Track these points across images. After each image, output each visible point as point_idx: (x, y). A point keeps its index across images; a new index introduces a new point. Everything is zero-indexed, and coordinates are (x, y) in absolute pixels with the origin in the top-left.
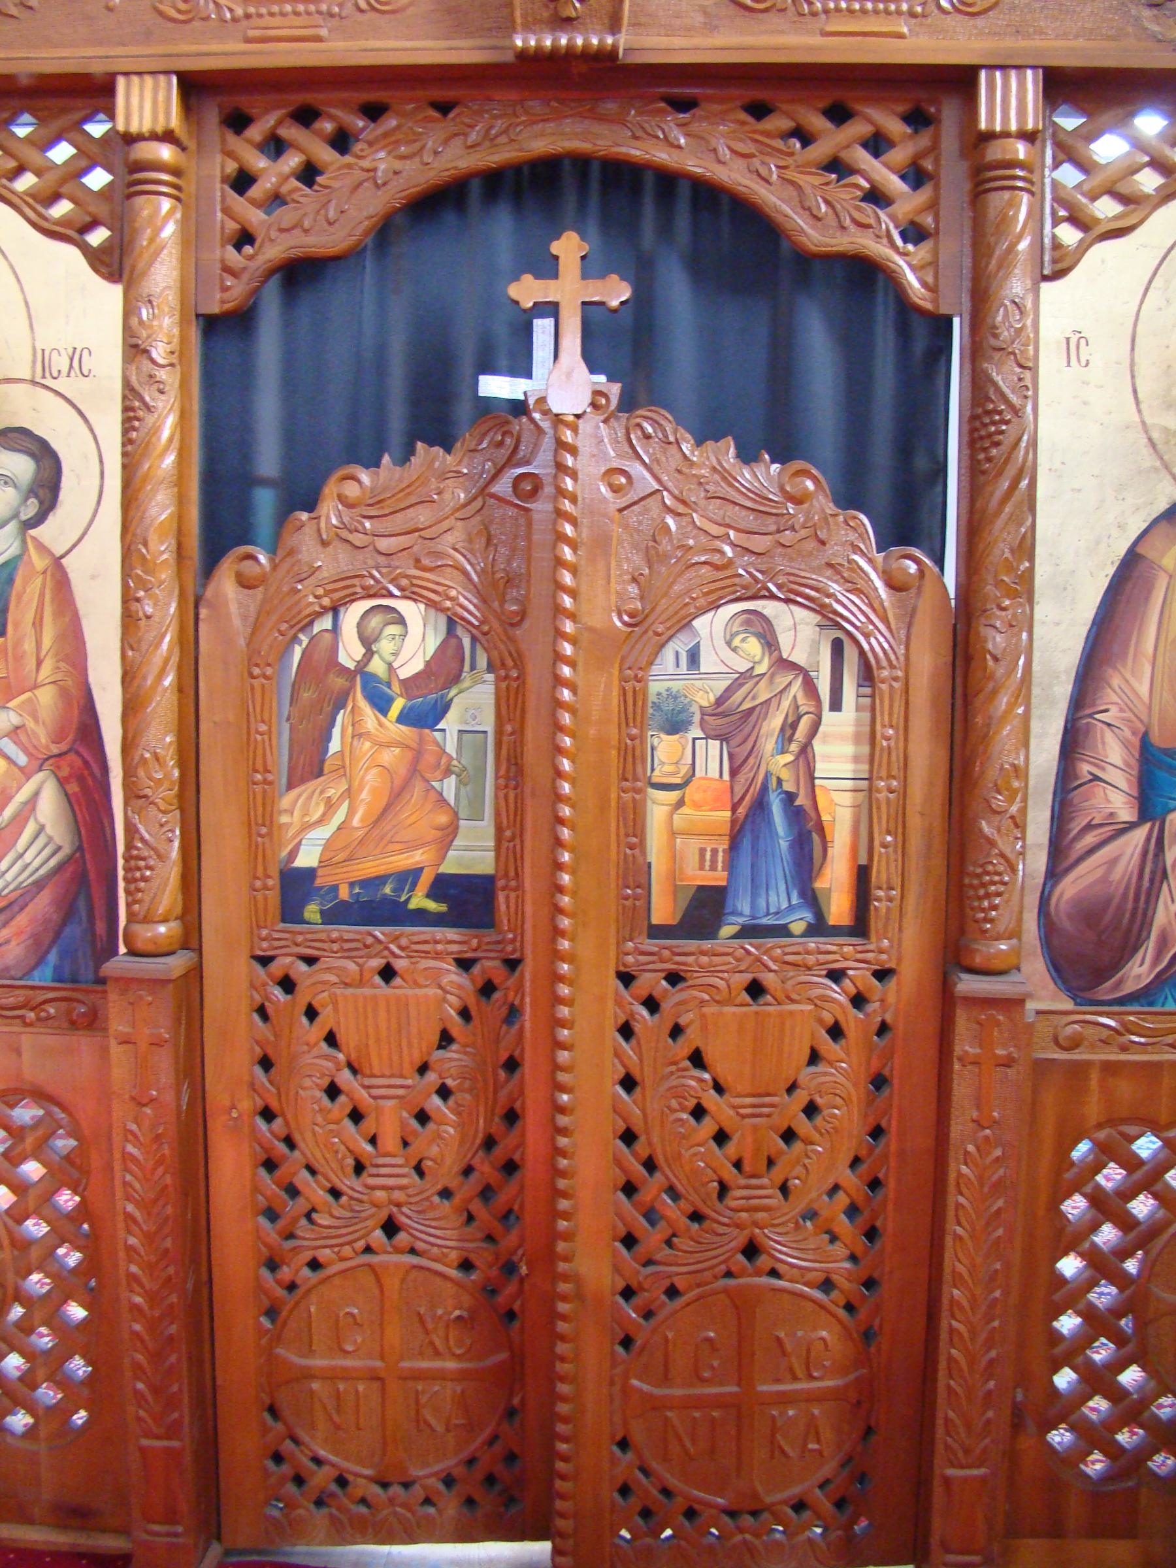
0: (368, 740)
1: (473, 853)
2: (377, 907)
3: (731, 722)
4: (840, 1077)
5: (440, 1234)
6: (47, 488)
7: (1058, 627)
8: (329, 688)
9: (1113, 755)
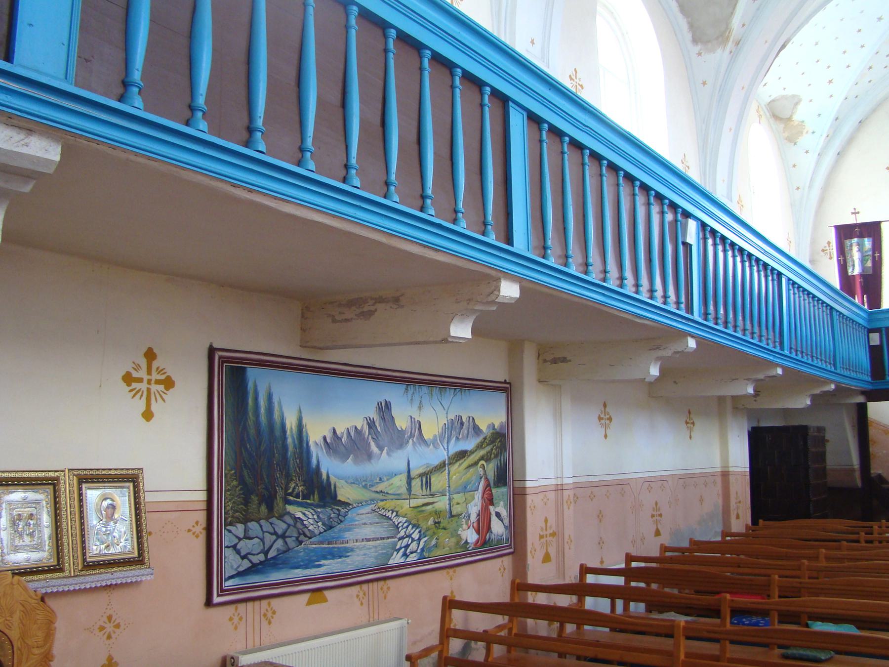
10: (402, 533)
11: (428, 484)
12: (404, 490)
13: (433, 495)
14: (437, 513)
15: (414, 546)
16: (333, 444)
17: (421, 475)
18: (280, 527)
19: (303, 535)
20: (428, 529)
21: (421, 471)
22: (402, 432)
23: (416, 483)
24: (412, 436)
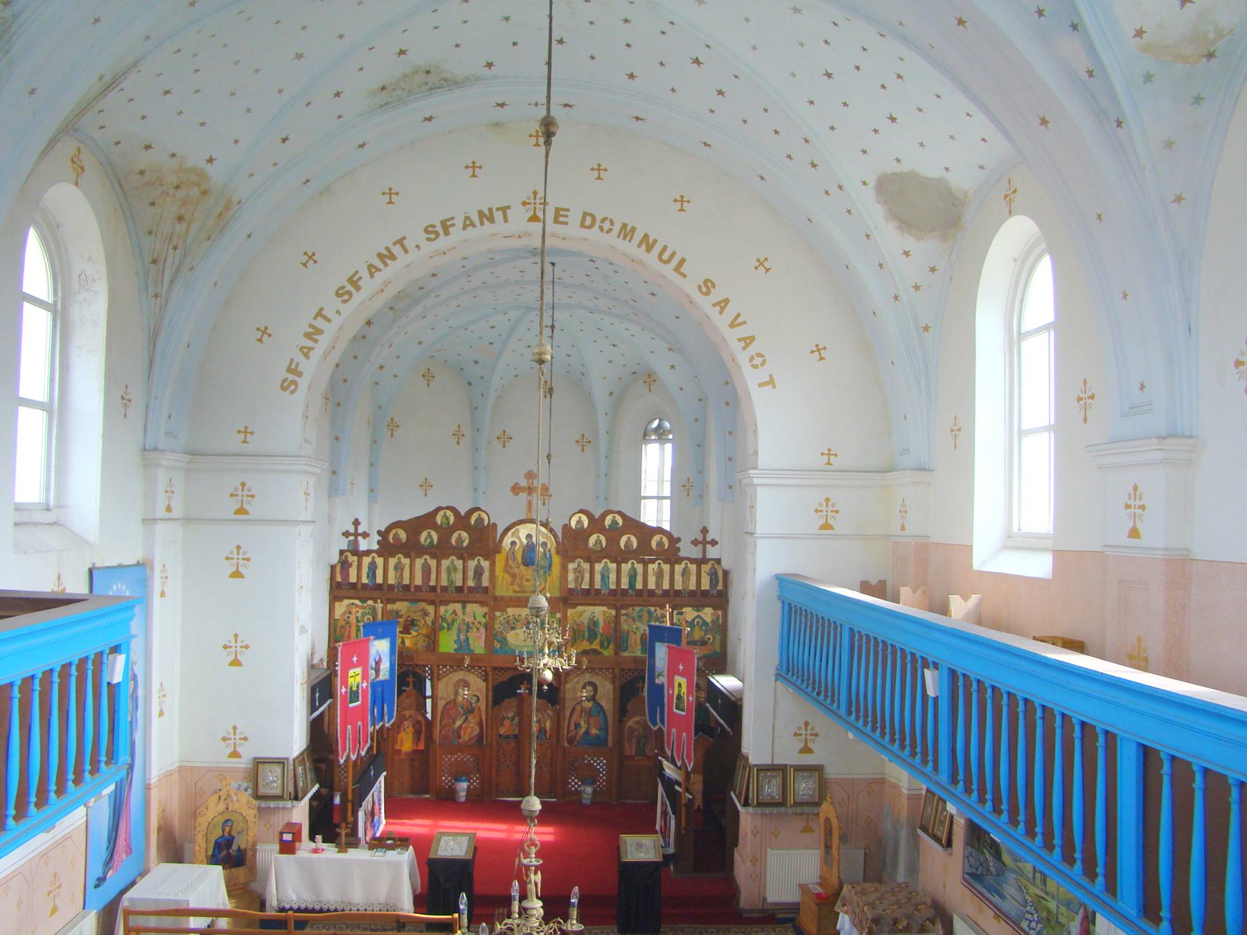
0: (507, 722)
2: (508, 737)
4: (549, 752)
6: (478, 700)
7: (568, 713)
8: (504, 718)
11: (1044, 882)
12: (1031, 876)
13: (1047, 893)
14: (1048, 910)
15: (1033, 924)
19: (988, 872)
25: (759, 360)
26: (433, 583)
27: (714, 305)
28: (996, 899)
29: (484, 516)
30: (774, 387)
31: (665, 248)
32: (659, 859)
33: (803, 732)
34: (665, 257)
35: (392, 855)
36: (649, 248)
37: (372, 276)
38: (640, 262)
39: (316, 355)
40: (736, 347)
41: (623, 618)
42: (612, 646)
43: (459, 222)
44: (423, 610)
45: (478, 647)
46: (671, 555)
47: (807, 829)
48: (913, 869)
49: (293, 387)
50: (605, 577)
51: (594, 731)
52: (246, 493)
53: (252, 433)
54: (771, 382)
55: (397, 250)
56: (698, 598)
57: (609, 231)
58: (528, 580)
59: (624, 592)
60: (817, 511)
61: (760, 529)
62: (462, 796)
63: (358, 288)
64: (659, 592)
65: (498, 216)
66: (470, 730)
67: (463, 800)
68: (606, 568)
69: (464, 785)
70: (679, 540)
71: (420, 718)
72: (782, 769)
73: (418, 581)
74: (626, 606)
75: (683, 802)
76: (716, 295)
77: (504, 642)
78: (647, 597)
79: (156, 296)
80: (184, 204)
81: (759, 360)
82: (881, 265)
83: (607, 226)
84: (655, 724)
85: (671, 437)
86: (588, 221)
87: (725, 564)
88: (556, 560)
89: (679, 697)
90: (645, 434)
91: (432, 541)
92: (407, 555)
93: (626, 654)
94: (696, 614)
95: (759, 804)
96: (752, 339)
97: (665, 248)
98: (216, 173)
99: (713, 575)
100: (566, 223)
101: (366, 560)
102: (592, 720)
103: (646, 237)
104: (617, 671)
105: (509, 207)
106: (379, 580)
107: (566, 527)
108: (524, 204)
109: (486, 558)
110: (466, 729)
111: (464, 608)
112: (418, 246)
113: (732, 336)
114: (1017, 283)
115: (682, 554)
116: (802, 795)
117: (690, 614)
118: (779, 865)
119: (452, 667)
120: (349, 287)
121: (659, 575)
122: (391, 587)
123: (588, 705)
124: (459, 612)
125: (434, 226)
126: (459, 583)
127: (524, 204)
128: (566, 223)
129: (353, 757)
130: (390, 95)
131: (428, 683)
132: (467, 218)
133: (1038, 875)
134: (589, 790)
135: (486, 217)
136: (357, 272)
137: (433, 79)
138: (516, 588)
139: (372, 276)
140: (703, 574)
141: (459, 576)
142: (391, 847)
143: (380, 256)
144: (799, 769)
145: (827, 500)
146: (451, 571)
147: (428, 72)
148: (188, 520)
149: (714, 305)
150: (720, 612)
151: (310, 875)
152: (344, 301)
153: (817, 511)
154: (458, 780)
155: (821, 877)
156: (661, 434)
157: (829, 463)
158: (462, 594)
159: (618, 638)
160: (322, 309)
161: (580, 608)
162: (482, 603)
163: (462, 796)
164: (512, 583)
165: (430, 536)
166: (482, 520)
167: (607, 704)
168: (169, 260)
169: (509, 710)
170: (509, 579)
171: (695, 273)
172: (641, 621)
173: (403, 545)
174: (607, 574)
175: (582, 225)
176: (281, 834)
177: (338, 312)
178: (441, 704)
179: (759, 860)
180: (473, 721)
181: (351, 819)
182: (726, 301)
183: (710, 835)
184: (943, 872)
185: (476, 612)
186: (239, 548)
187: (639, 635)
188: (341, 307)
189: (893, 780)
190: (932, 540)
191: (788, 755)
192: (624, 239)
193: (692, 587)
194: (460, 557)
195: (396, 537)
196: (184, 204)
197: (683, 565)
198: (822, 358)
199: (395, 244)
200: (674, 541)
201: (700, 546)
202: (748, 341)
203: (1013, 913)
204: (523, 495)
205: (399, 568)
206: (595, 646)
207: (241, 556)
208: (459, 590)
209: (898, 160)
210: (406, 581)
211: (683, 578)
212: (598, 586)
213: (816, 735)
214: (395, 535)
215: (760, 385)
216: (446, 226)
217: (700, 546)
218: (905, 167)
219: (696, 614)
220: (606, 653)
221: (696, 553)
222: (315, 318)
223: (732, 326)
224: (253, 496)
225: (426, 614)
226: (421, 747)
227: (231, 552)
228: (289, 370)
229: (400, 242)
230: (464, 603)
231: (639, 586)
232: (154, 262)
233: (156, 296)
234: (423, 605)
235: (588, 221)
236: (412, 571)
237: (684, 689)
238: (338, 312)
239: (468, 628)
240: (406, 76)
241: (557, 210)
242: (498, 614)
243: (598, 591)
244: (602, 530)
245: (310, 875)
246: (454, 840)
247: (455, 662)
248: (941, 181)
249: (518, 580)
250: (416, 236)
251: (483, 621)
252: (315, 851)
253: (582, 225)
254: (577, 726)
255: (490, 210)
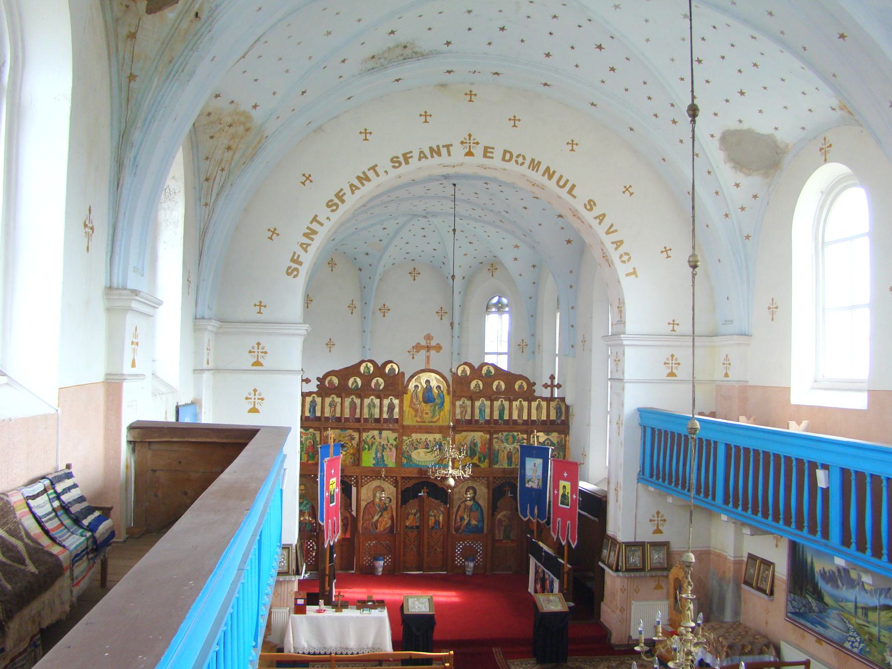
0: (411, 517)
1: (418, 524)
2: (412, 528)
3: (434, 516)
4: (441, 538)
5: (415, 549)
9: (458, 518)
10: (851, 634)
11: (866, 615)
12: (853, 611)
13: (869, 622)
14: (870, 634)
15: (856, 644)
16: (823, 574)
17: (862, 608)
18: (804, 602)
19: (811, 610)
20: (865, 640)
21: (863, 605)
22: (853, 581)
23: (860, 611)
24: (858, 584)
25: (626, 257)
26: (358, 416)
27: (595, 218)
28: (819, 629)
29: (395, 367)
30: (637, 276)
31: (561, 177)
32: (567, 610)
33: (656, 518)
34: (561, 183)
35: (375, 613)
36: (550, 177)
37: (353, 192)
38: (543, 188)
39: (312, 250)
40: (610, 248)
41: (495, 440)
42: (487, 461)
43: (416, 155)
44: (350, 435)
45: (391, 462)
46: (529, 396)
47: (658, 587)
48: (737, 612)
49: (295, 273)
50: (482, 411)
51: (474, 522)
52: (260, 350)
53: (265, 306)
54: (634, 273)
55: (371, 174)
56: (547, 426)
57: (522, 164)
58: (427, 413)
59: (496, 422)
60: (665, 363)
61: (627, 377)
62: (380, 571)
63: (343, 201)
64: (520, 421)
65: (444, 151)
66: (384, 523)
67: (380, 574)
68: (483, 404)
69: (382, 563)
70: (534, 384)
71: (348, 515)
72: (642, 545)
73: (347, 414)
74: (497, 432)
75: (566, 570)
76: (597, 211)
77: (409, 458)
78: (511, 425)
79: (206, 205)
80: (233, 137)
81: (626, 257)
82: (717, 193)
83: (520, 160)
84: (525, 516)
85: (507, 309)
86: (507, 156)
87: (568, 401)
88: (448, 399)
89: (564, 495)
90: (487, 308)
91: (357, 385)
92: (339, 396)
93: (496, 466)
94: (546, 437)
95: (627, 570)
96: (621, 242)
97: (561, 177)
98: (257, 116)
99: (558, 410)
100: (492, 158)
101: (308, 399)
102: (472, 514)
103: (548, 169)
104: (491, 479)
105: (451, 145)
106: (318, 414)
107: (455, 375)
108: (462, 143)
109: (397, 397)
110: (381, 522)
111: (380, 433)
112: (386, 172)
113: (608, 240)
114: (822, 208)
115: (536, 394)
116: (653, 563)
117: (542, 437)
118: (637, 613)
119: (371, 477)
120: (336, 201)
121: (521, 409)
122: (327, 419)
123: (469, 503)
124: (377, 438)
125: (398, 157)
126: (377, 416)
127: (462, 143)
128: (492, 158)
129: (332, 543)
130: (377, 63)
131: (354, 489)
132: (421, 152)
133: (860, 611)
134: (471, 565)
135: (435, 151)
136: (342, 190)
137: (408, 52)
138: (419, 419)
139: (353, 192)
140: (551, 409)
141: (377, 410)
142: (374, 607)
143: (359, 178)
144: (654, 545)
145: (672, 356)
146: (372, 407)
147: (405, 47)
148: (217, 370)
149: (595, 218)
150: (563, 436)
151: (318, 630)
152: (333, 211)
153: (665, 363)
154: (377, 559)
155: (670, 620)
156: (500, 307)
157: (673, 330)
158: (379, 424)
159: (491, 455)
160: (316, 216)
161: (464, 434)
162: (393, 430)
163: (380, 571)
164: (416, 416)
165: (355, 381)
166: (394, 370)
167: (483, 502)
168: (218, 178)
169: (413, 508)
170: (414, 413)
171: (582, 195)
172: (507, 443)
173: (335, 388)
174: (483, 408)
175: (503, 159)
176: (296, 599)
177: (328, 218)
178: (363, 504)
179: (625, 610)
180: (386, 516)
181: (327, 588)
182: (604, 215)
183: (586, 593)
184: (768, 613)
185: (389, 436)
186: (255, 390)
187: (506, 453)
188: (331, 215)
189: (718, 551)
190: (750, 384)
191: (646, 535)
192: (533, 170)
193: (544, 417)
194: (378, 397)
195: (330, 382)
196: (233, 137)
197: (537, 402)
198: (668, 257)
199: (369, 170)
200: (531, 385)
201: (549, 388)
202: (618, 244)
203: (836, 638)
204: (423, 352)
205: (332, 405)
206: (475, 460)
207: (257, 397)
208: (377, 421)
209: (740, 121)
210: (338, 415)
211: (538, 412)
212: (477, 417)
213: (665, 521)
214: (330, 381)
215: (627, 275)
216: (407, 157)
217: (549, 388)
218: (745, 126)
219: (546, 437)
220: (482, 465)
221: (546, 393)
222: (311, 223)
223: (608, 233)
224: (266, 353)
225: (352, 439)
226: (348, 536)
227: (250, 394)
228: (293, 260)
229: (373, 168)
230: (381, 430)
231: (506, 417)
232: (207, 180)
233: (206, 205)
234: (350, 432)
235: (508, 156)
236: (342, 407)
237: (568, 490)
238: (328, 218)
239: (384, 448)
240: (389, 49)
241: (486, 148)
242: (405, 438)
243: (477, 421)
244: (480, 377)
245: (318, 630)
246: (419, 603)
247: (374, 473)
248: (770, 136)
249: (419, 414)
250: (384, 164)
251: (395, 443)
252: (319, 611)
253: (503, 159)
254: (462, 518)
255: (438, 147)
